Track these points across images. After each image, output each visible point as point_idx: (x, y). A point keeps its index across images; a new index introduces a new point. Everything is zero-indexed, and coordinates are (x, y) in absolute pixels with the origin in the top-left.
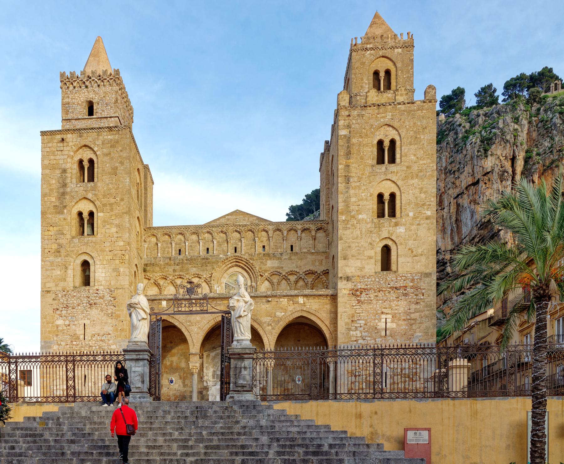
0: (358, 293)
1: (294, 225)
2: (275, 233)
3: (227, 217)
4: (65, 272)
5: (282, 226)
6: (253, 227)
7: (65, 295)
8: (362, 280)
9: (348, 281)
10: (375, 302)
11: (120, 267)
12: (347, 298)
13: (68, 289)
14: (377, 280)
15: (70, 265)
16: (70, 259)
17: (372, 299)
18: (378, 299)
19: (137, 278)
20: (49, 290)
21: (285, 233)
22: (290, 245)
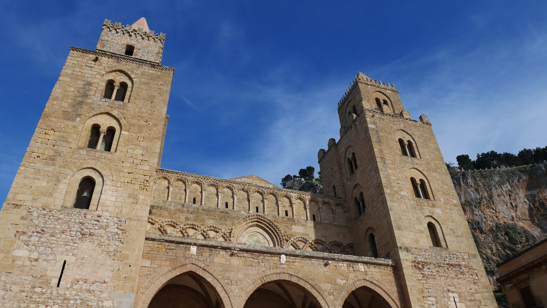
1: (315, 197)
3: (243, 179)
6: (275, 191)
11: (139, 193)
13: (52, 207)
14: (434, 255)
15: (65, 178)
16: (68, 170)
17: (435, 274)
20: (19, 203)
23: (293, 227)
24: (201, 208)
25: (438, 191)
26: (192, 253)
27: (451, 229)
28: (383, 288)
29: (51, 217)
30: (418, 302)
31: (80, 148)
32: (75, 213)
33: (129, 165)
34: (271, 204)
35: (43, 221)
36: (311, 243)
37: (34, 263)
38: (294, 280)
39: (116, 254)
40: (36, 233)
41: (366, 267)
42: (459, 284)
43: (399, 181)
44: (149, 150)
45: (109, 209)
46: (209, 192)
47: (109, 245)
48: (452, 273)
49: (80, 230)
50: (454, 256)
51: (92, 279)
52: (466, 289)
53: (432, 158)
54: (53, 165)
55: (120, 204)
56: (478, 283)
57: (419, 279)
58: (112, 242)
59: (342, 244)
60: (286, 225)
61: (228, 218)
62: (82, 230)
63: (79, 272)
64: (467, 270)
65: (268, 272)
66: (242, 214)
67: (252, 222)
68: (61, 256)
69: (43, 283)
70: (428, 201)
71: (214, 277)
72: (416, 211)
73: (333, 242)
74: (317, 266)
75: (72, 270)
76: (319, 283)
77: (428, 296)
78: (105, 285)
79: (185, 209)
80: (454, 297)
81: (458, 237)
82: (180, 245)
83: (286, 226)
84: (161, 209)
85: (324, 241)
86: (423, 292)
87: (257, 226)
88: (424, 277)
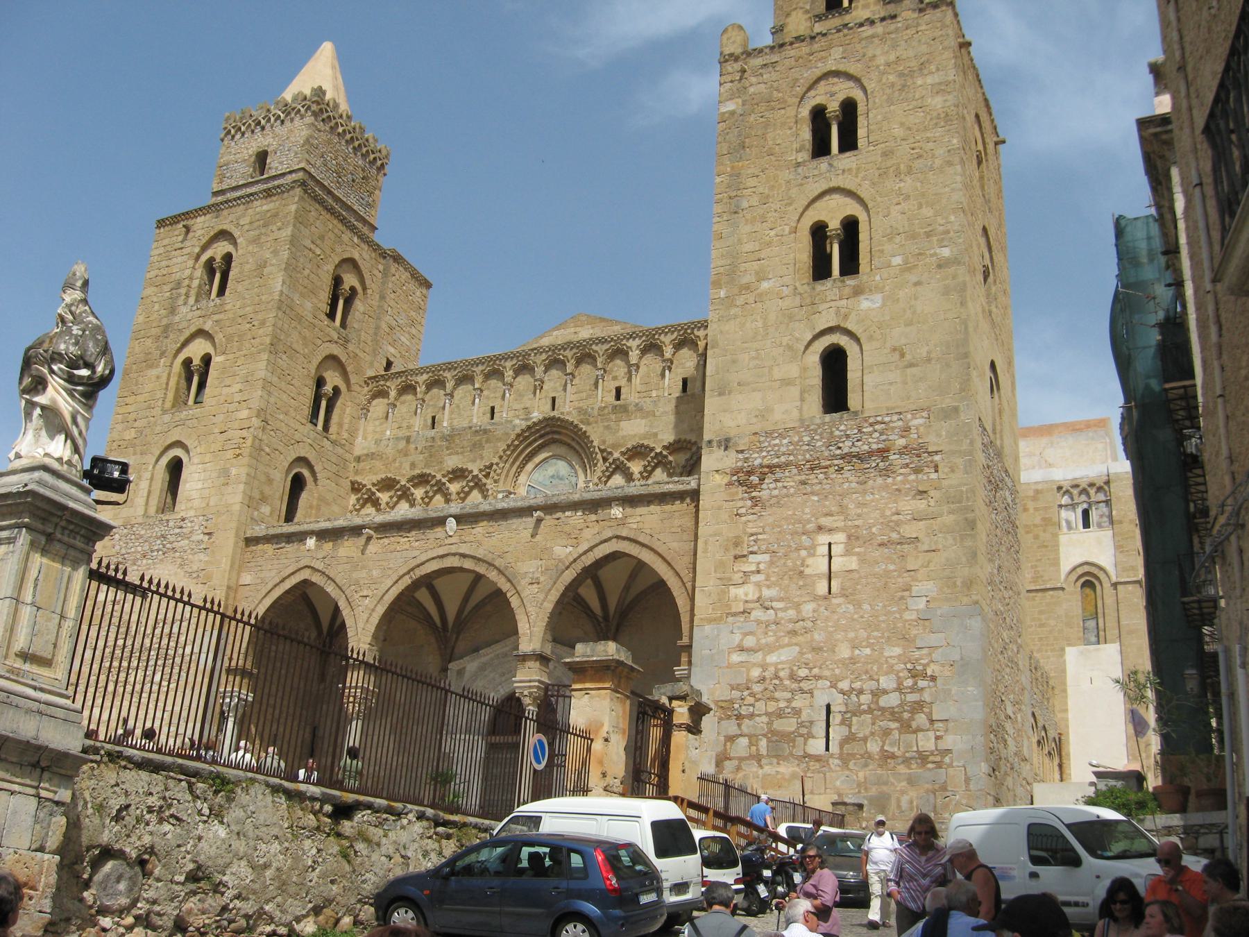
0: (755, 479)
1: (689, 331)
8: (766, 444)
23: (623, 424)
27: (894, 350)
28: (659, 550)
30: (715, 571)
31: (164, 412)
42: (860, 505)
48: (849, 480)
50: (877, 427)
52: (883, 516)
53: (909, 129)
54: (135, 454)
56: (932, 493)
61: (487, 442)
65: (423, 558)
66: (514, 426)
67: (541, 437)
79: (412, 446)
80: (830, 544)
81: (911, 365)
83: (607, 427)
85: (693, 440)
87: (554, 441)
88: (752, 507)
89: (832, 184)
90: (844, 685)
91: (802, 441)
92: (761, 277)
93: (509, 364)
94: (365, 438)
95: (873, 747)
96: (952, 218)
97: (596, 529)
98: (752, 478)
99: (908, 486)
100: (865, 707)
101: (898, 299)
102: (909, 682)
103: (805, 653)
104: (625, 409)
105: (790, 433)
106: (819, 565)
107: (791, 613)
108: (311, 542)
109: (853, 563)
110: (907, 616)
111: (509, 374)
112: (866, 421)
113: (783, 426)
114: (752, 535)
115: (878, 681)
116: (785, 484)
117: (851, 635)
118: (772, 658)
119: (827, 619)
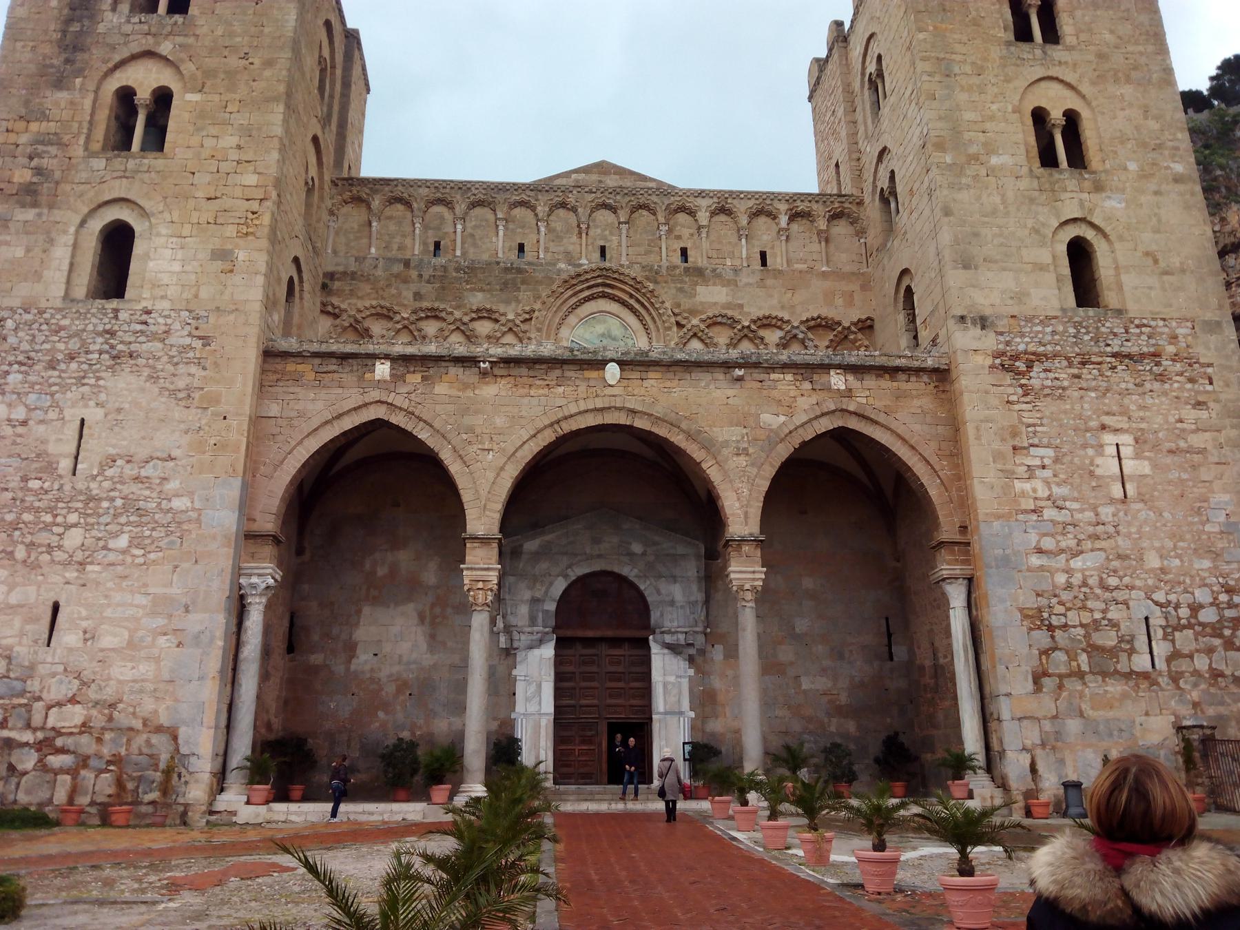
1: (768, 202)
2: (717, 218)
3: (574, 176)
4: (45, 251)
5: (735, 202)
6: (654, 198)
7: (29, 325)
8: (1028, 330)
9: (983, 328)
10: (1076, 394)
12: (991, 379)
13: (43, 305)
14: (1072, 330)
15: (65, 232)
17: (1066, 383)
18: (1084, 385)
19: (297, 299)
21: (744, 221)
22: (758, 250)
23: (699, 289)
24: (453, 265)
25: (1122, 143)
26: (377, 378)
27: (1147, 254)
28: (899, 431)
29: (44, 327)
32: (94, 311)
33: (208, 178)
34: (641, 234)
35: (28, 338)
36: (748, 327)
37: (20, 430)
38: (640, 423)
39: (192, 395)
40: (16, 366)
41: (850, 378)
42: (1142, 408)
43: (988, 126)
44: (254, 133)
45: (169, 293)
46: (473, 223)
47: (174, 375)
48: (1123, 377)
49: (106, 347)
50: (1143, 329)
51: (143, 453)
53: (1120, 38)
54: (35, 205)
55: (193, 277)
56: (1211, 404)
57: (1008, 402)
58: (182, 369)
59: (839, 323)
60: (679, 285)
61: (523, 282)
62: (112, 347)
63: (114, 441)
64: (1178, 367)
65: (573, 409)
66: (559, 271)
67: (589, 288)
68: (73, 411)
69: (41, 470)
70: (1081, 174)
71: (435, 430)
72: (1034, 207)
73: (813, 319)
74: (707, 385)
75: (99, 438)
76: (710, 426)
77: (1032, 445)
78: (171, 464)
79: (414, 274)
80: (1117, 445)
81: (1166, 273)
82: (350, 361)
83: (681, 290)
84: (353, 279)
85: (786, 318)
86: (1014, 434)
87: (604, 296)
88: (1026, 395)
89: (1050, 73)
90: (1160, 596)
91: (1067, 332)
92: (990, 149)
93: (543, 198)
94: (335, 252)
95: (1201, 663)
96: (1179, 136)
97: (813, 400)
98: (1017, 364)
99: (1186, 394)
100: (1183, 622)
101: (1141, 205)
102: (1223, 597)
103: (1112, 560)
104: (699, 273)
105: (1053, 321)
106: (1108, 466)
107: (1089, 515)
108: (383, 370)
109: (1145, 468)
110: (1208, 528)
111: (542, 210)
112: (1132, 322)
113: (1043, 313)
114: (1029, 426)
115: (1193, 594)
116: (1057, 375)
117: (1157, 544)
118: (1077, 563)
119: (1129, 524)
